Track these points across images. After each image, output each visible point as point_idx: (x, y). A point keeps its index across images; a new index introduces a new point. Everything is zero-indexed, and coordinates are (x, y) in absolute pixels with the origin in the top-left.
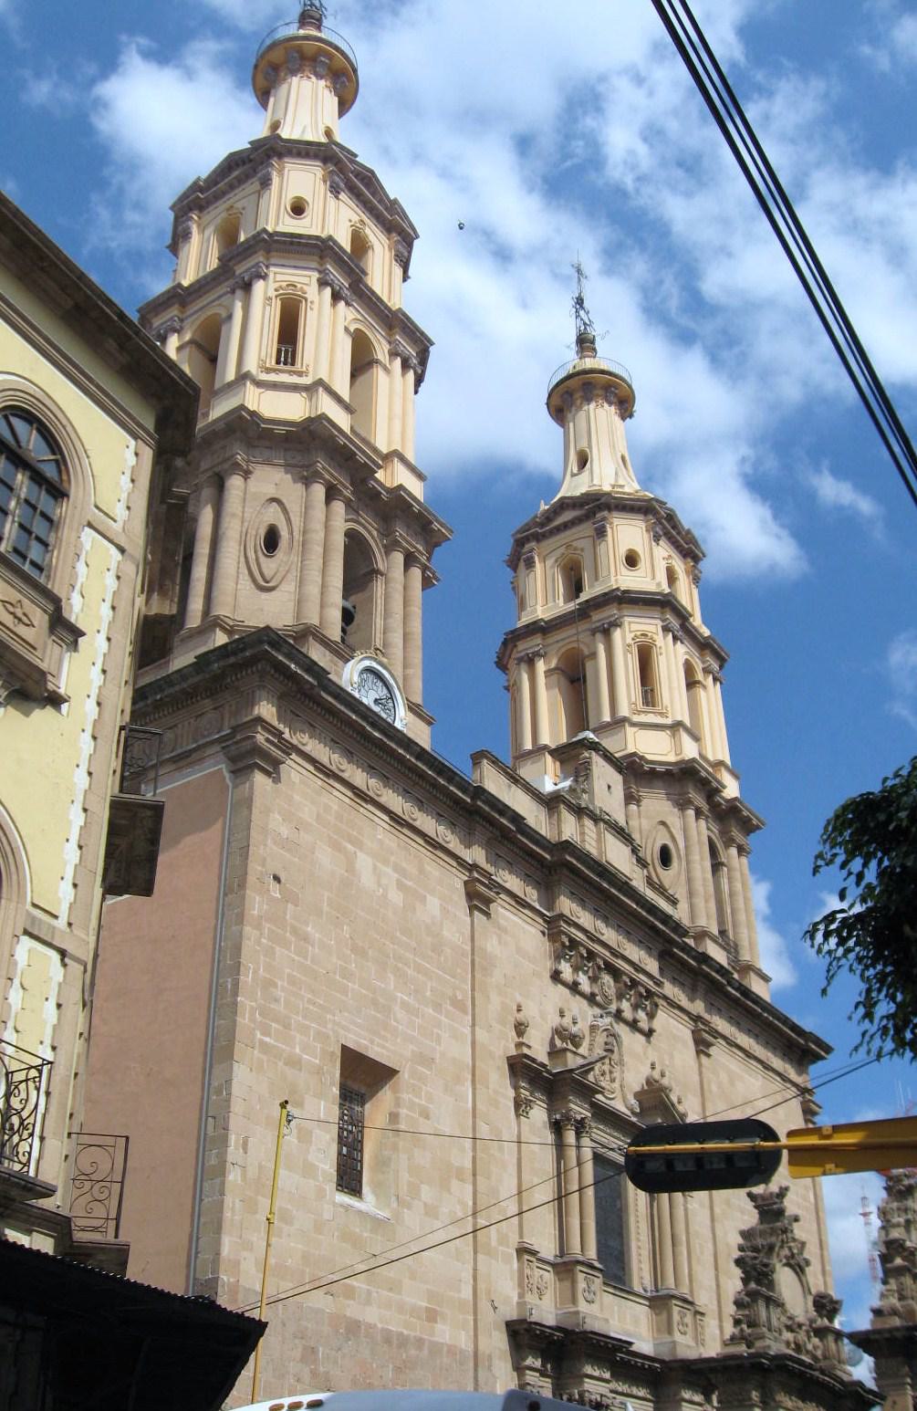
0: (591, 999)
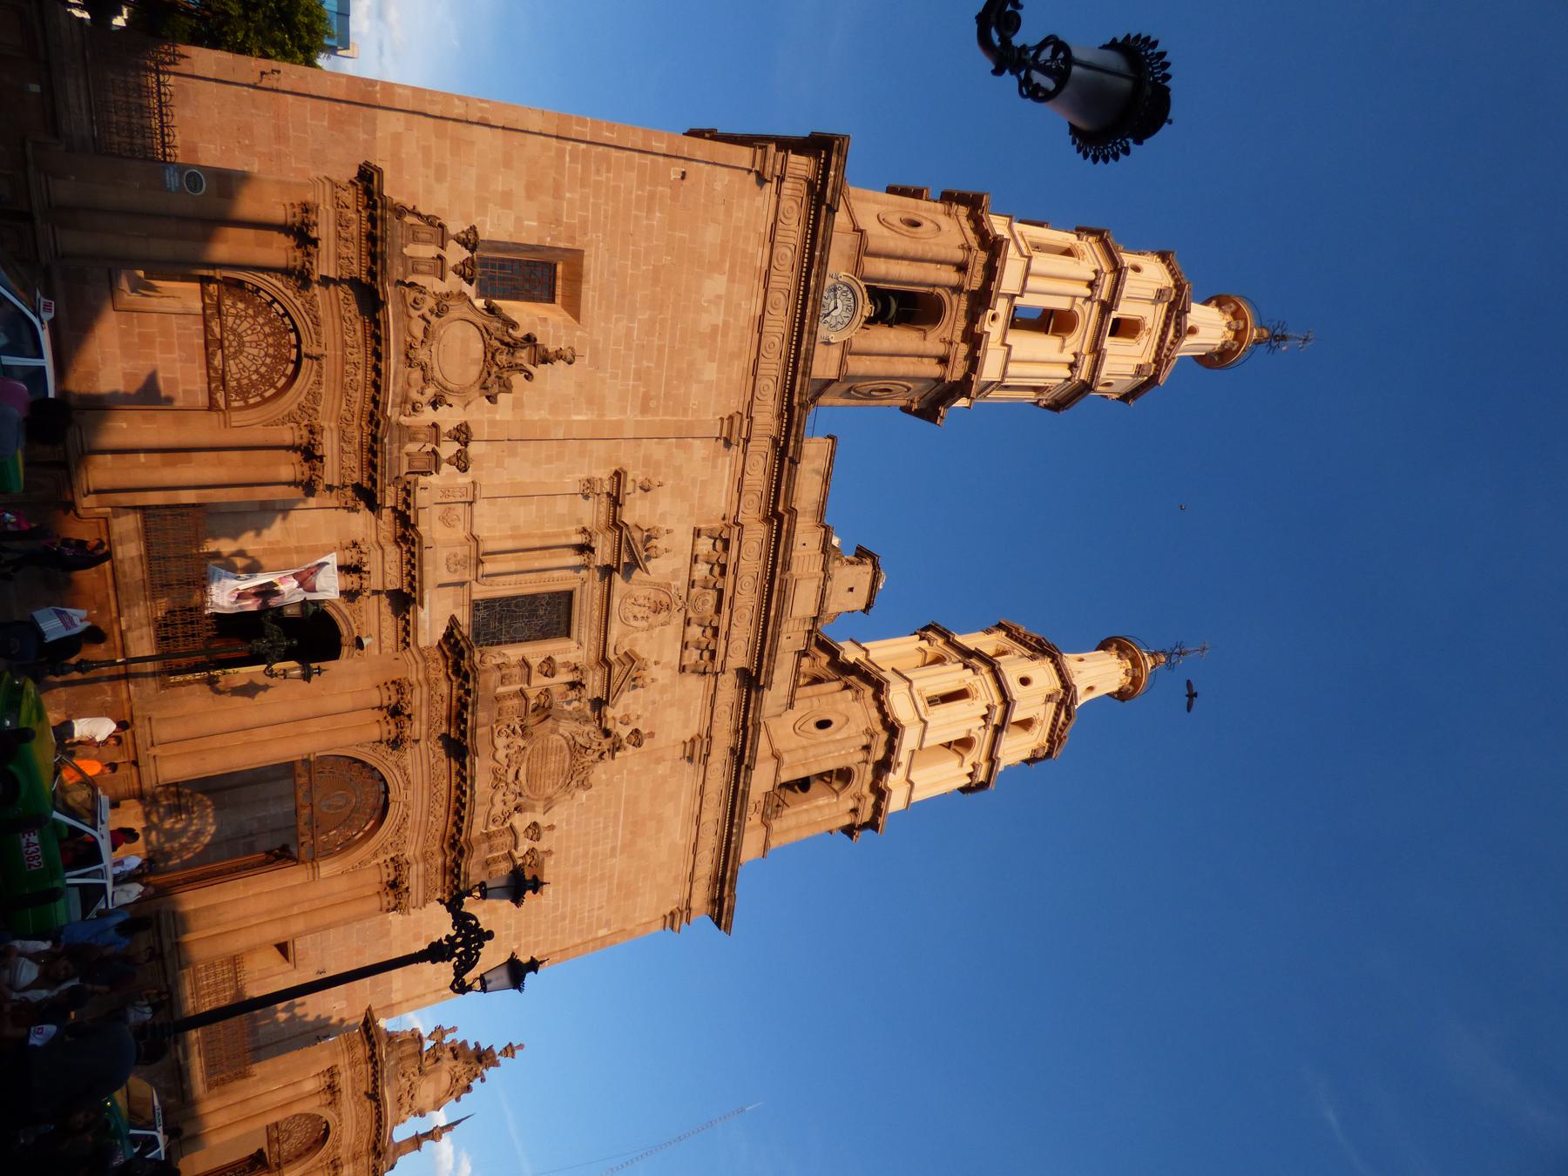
0: (692, 584)
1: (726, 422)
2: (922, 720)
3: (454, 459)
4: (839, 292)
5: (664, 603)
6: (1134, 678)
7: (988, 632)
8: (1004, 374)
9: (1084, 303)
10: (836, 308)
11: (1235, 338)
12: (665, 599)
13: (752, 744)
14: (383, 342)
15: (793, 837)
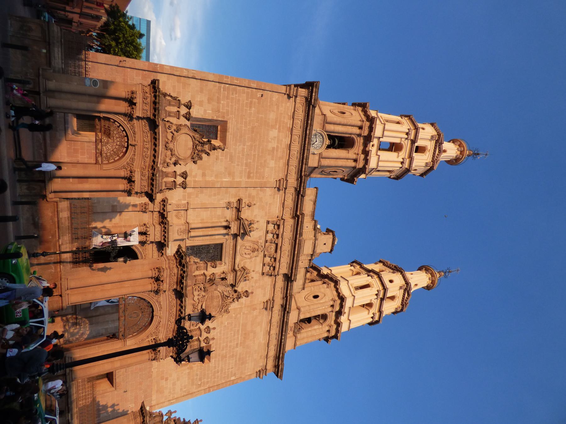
0: (266, 241)
1: (278, 182)
2: (353, 295)
3: (181, 184)
4: (317, 136)
5: (256, 248)
6: (432, 281)
7: (376, 263)
8: (378, 166)
9: (405, 140)
10: (316, 141)
11: (461, 154)
12: (256, 247)
13: (289, 303)
14: (157, 140)
15: (305, 341)
